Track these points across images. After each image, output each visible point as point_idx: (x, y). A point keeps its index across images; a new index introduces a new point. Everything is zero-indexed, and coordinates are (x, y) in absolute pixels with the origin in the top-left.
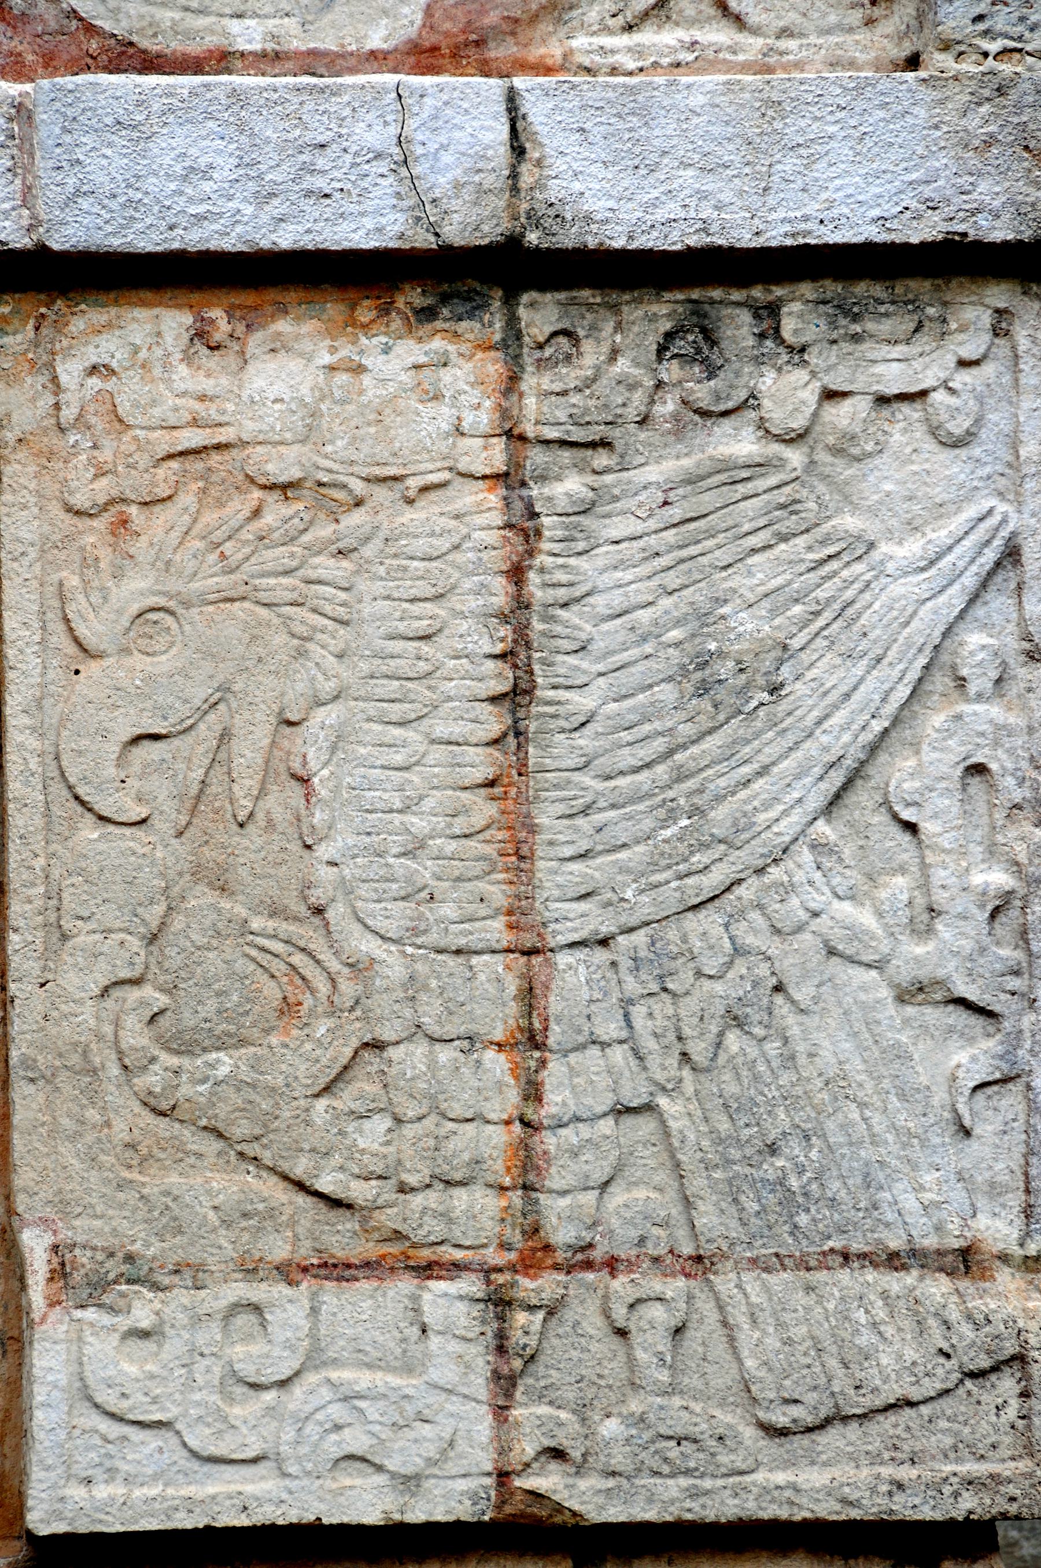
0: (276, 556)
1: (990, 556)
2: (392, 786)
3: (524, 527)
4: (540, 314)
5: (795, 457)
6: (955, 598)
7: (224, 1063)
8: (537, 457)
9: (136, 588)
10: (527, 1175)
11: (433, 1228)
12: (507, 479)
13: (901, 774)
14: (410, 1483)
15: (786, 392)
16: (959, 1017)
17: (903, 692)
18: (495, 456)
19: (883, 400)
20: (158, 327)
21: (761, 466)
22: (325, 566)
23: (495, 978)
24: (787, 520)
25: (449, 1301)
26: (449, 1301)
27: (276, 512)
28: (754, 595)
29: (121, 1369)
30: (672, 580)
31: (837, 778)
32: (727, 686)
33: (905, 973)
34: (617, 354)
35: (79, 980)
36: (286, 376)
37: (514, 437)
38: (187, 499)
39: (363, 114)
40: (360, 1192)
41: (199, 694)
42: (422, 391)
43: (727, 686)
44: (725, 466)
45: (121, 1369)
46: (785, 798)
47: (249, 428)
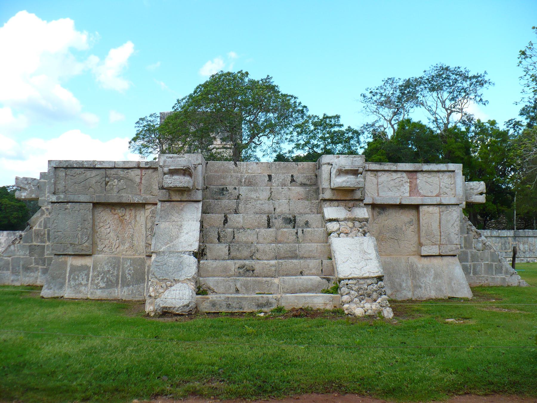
2: (435, 225)
3: (440, 215)
4: (441, 206)
10: (440, 241)
15: (450, 210)
20: (426, 207)
23: (439, 233)
24: (450, 215)
25: (437, 246)
26: (437, 246)
28: (449, 218)
29: (425, 249)
32: (448, 221)
34: (443, 208)
35: (423, 233)
36: (431, 209)
39: (435, 199)
42: (436, 209)
43: (448, 221)
45: (425, 249)
46: (450, 226)
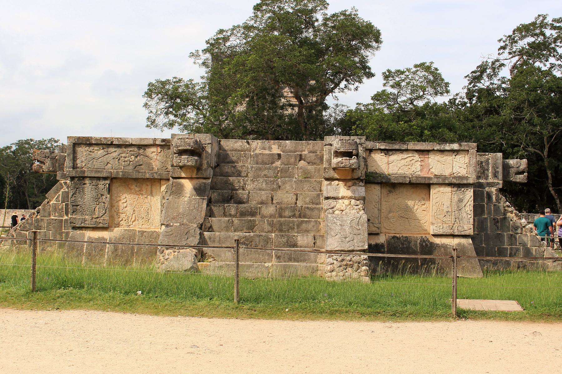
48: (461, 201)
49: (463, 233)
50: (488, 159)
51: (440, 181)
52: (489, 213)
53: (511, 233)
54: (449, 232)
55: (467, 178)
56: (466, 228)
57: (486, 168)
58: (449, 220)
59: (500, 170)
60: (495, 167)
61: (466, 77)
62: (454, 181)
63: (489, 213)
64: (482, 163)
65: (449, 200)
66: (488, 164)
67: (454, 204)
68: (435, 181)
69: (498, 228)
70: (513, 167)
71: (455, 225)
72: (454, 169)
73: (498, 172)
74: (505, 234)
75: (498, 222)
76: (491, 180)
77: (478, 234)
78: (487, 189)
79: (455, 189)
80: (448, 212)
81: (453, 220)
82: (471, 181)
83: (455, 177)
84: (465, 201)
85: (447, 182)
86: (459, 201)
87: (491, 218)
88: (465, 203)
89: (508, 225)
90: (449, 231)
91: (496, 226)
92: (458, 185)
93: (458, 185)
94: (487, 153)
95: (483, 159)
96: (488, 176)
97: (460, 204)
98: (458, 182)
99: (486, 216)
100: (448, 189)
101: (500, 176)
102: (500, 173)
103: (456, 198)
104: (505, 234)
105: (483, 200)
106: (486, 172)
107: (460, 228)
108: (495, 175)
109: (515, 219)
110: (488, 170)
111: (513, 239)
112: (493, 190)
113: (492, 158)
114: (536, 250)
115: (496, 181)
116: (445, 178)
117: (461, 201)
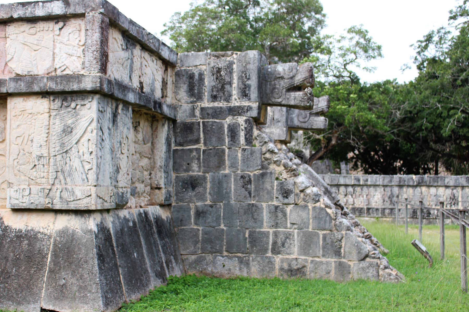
0: (29, 120)
1: (91, 120)
5: (74, 111)
6: (88, 124)
7: (23, 166)
8: (51, 111)
9: (18, 123)
11: (40, 182)
12: (49, 112)
13: (82, 140)
14: (37, 205)
16: (87, 163)
17: (83, 132)
18: (48, 111)
19: (82, 105)
21: (70, 111)
22: (33, 121)
27: (30, 116)
30: (62, 122)
31: (76, 141)
33: (82, 159)
37: (49, 109)
38: (22, 115)
40: (34, 178)
41: (22, 133)
44: (68, 111)
47: (27, 108)
48: (68, 131)
49: (72, 206)
50: (231, 63)
51: (23, 87)
52: (233, 165)
53: (275, 203)
54: (42, 202)
55: (78, 78)
56: (79, 194)
57: (227, 79)
58: (44, 175)
59: (253, 82)
60: (244, 77)
61: (411, 46)
62: (52, 86)
63: (233, 165)
64: (219, 70)
65: (45, 131)
66: (231, 73)
67: (54, 138)
68: (11, 87)
69: (250, 193)
70: (282, 78)
71: (54, 188)
72: (56, 60)
73: (249, 86)
74: (264, 205)
75: (250, 182)
76: (236, 101)
77: (211, 206)
78: (229, 120)
79: (58, 103)
80: (40, 157)
81: (52, 175)
82: (88, 85)
83: (51, 79)
84: (78, 132)
85: (36, 88)
86: (64, 131)
87: (236, 175)
88: (78, 137)
89: (269, 188)
90: (42, 200)
91: (246, 189)
92: (64, 93)
93: (64, 93)
94: (229, 53)
95: (222, 63)
96: (230, 95)
97: (66, 139)
98: (59, 88)
99: (227, 171)
100: (42, 105)
101: (254, 93)
102: (252, 88)
103: (58, 126)
104: (264, 205)
105: (221, 140)
106: (227, 87)
107: (65, 195)
108: (244, 94)
109: (285, 175)
110: (230, 84)
111: (280, 214)
112: (241, 120)
113: (239, 61)
114: (325, 237)
115: (246, 103)
116: (33, 78)
117: (68, 131)
